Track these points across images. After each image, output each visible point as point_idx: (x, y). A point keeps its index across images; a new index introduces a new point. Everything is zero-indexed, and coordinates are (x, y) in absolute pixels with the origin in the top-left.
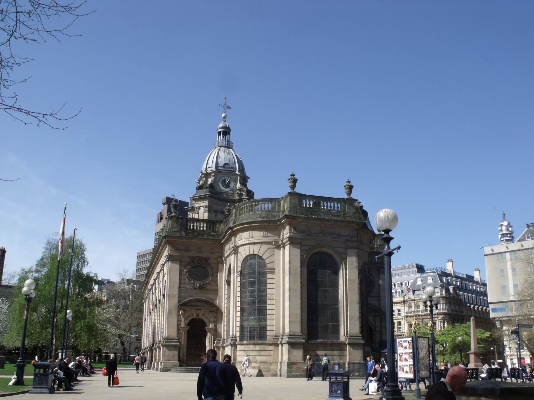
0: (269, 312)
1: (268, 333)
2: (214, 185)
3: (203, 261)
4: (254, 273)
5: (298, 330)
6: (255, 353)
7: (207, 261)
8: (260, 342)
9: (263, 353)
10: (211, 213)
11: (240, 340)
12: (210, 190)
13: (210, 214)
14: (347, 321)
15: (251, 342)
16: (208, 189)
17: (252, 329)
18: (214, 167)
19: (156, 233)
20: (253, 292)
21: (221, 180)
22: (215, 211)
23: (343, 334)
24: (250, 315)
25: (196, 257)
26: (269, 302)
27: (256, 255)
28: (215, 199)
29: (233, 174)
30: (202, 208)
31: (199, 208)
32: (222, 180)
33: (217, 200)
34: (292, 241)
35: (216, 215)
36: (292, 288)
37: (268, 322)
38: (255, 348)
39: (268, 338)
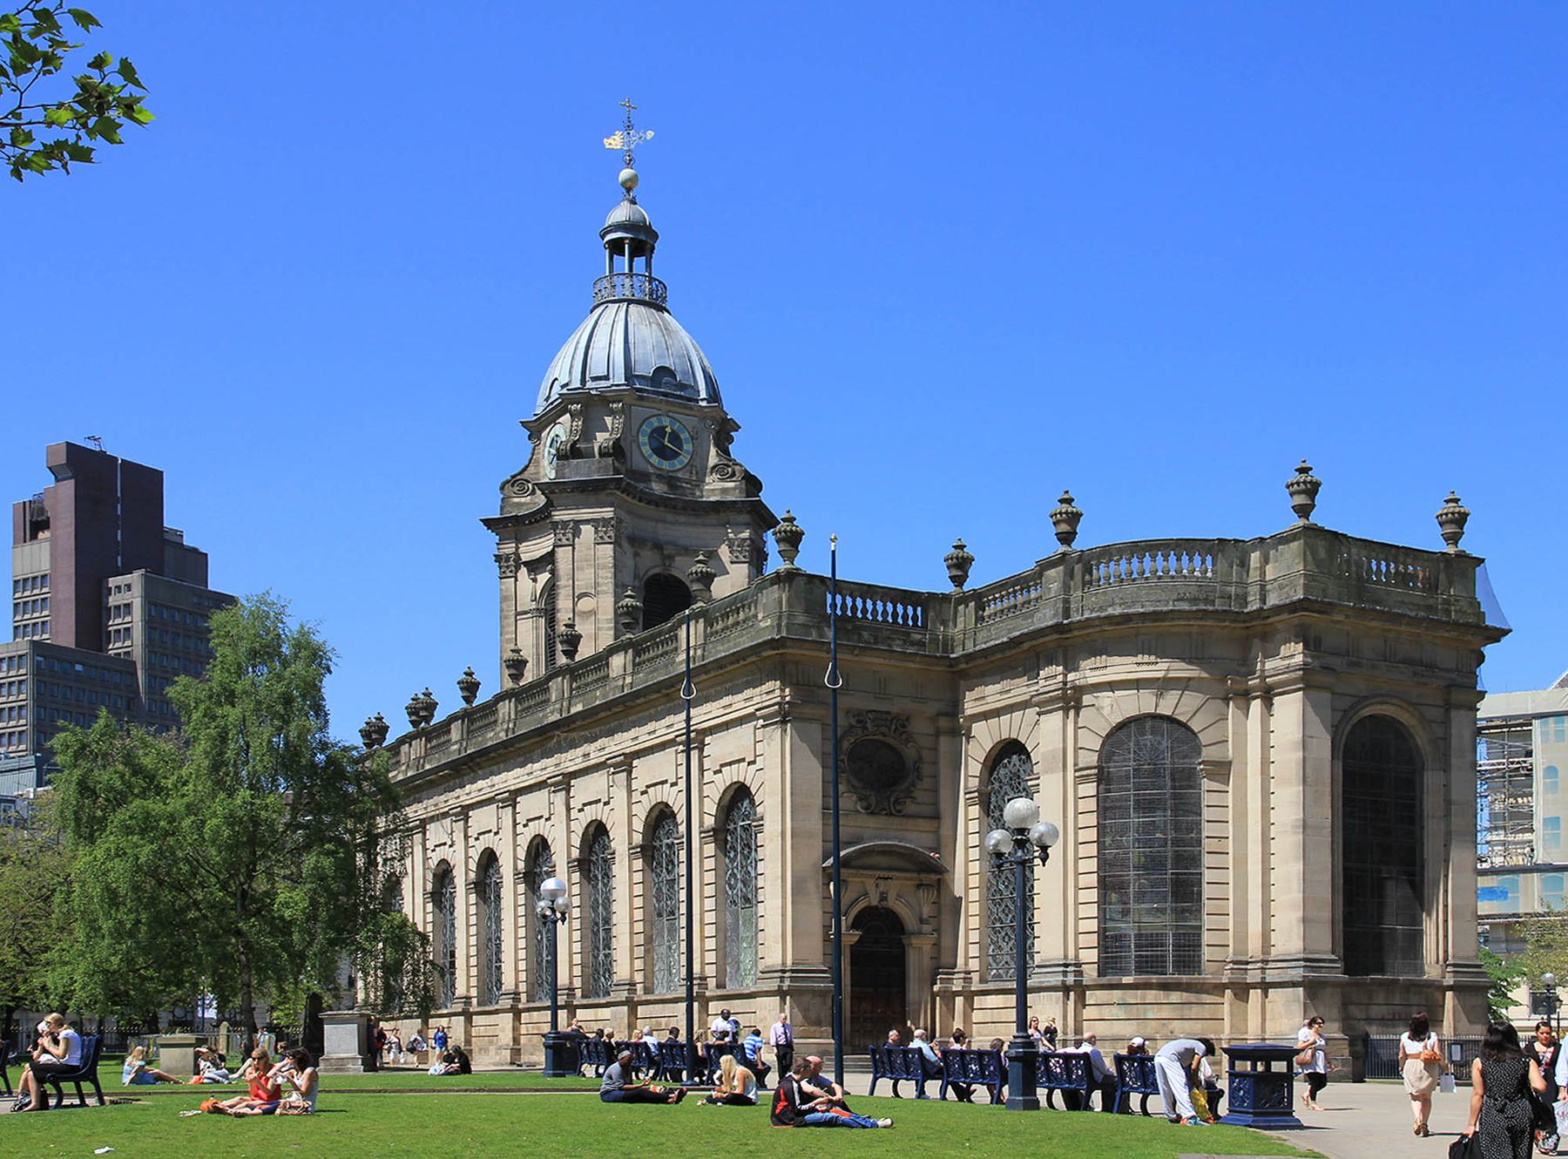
0: (1207, 891)
1: (1207, 953)
2: (622, 443)
3: (894, 727)
4: (1156, 773)
5: (1324, 945)
6: (1165, 1012)
7: (904, 726)
8: (1185, 978)
9: (1195, 1011)
10: (620, 546)
11: (1099, 973)
12: (616, 464)
13: (618, 548)
14: (1446, 921)
15: (1154, 978)
16: (610, 460)
17: (1149, 941)
18: (619, 378)
19: (16, 582)
20: (1149, 828)
21: (647, 429)
22: (632, 540)
23: (1434, 959)
24: (1141, 896)
25: (870, 711)
26: (1207, 860)
27: (1162, 717)
28: (634, 497)
29: (691, 408)
30: (587, 529)
31: (578, 523)
32: (649, 431)
33: (640, 501)
34: (1308, 680)
35: (636, 555)
36: (1309, 821)
37: (1208, 922)
38: (1168, 996)
39: (1205, 965)
